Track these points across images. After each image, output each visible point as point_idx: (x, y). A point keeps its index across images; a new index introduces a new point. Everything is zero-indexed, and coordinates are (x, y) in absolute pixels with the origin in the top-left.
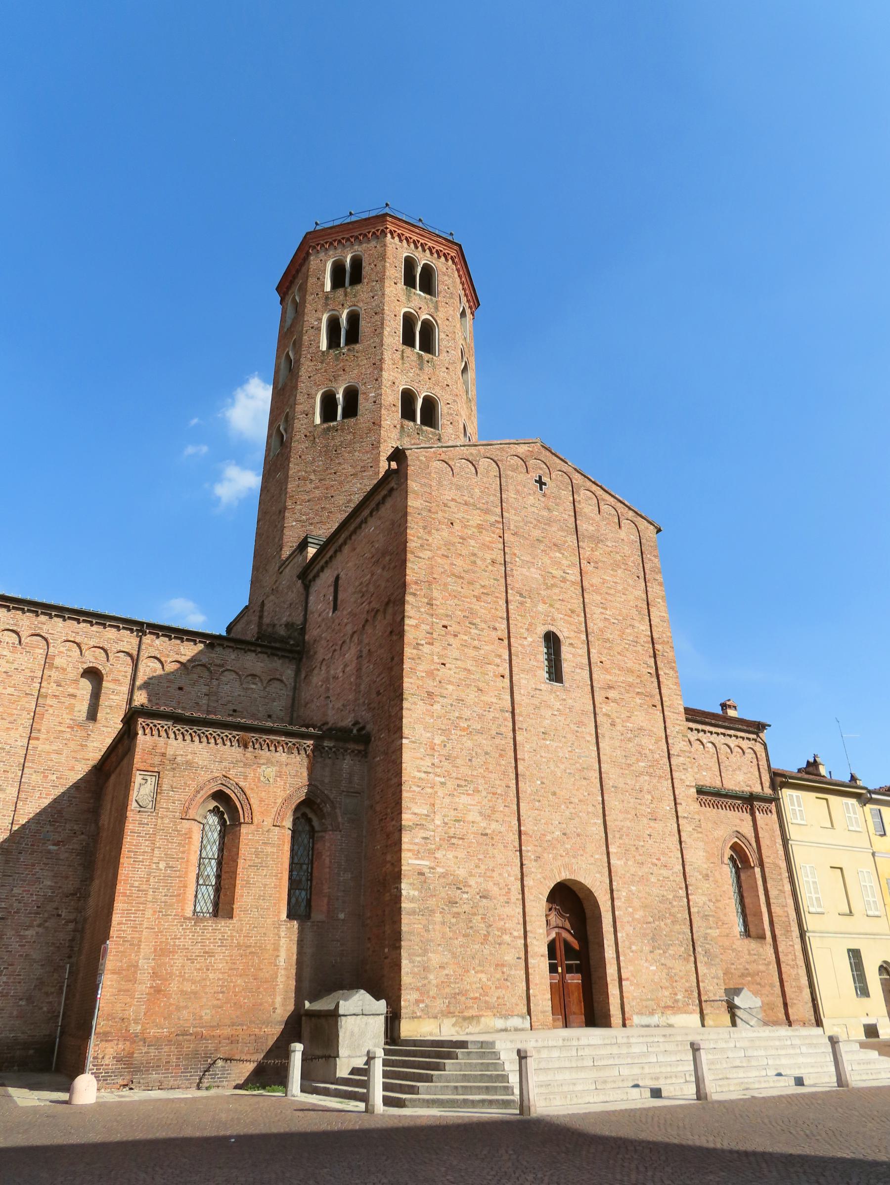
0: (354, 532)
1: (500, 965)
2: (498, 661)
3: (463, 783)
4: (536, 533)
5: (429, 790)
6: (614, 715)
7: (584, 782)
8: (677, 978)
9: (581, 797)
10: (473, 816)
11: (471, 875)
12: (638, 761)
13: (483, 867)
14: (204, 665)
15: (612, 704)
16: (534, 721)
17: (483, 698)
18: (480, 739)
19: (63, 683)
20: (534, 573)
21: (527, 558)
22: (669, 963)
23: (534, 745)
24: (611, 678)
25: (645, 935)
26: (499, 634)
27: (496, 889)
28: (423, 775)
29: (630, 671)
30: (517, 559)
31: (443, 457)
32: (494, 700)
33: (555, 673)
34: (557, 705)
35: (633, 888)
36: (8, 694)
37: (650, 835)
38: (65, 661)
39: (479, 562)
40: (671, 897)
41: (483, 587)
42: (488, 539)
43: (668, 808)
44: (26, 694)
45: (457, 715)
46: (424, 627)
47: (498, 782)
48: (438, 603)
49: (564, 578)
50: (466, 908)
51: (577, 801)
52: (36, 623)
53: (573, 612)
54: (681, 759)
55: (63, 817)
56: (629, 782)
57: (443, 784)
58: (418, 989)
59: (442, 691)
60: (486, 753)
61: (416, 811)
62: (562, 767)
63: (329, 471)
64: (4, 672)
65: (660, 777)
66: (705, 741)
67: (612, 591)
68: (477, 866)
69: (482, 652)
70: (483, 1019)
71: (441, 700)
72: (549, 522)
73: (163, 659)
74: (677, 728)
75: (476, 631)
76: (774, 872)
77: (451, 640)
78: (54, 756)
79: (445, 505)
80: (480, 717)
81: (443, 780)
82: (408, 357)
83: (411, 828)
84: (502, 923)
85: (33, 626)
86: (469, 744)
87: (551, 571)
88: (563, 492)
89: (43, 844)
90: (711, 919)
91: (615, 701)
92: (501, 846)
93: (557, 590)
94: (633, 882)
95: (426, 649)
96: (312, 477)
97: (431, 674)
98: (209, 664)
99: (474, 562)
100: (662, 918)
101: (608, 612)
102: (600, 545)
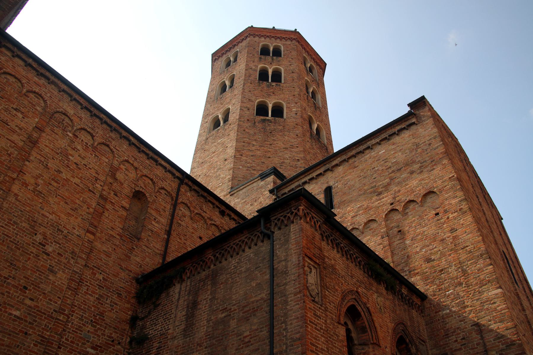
0: (354, 156)
14: (217, 226)
19: (119, 195)
36: (75, 183)
38: (123, 177)
44: (89, 190)
52: (108, 135)
55: (104, 320)
63: (267, 143)
64: (75, 163)
73: (192, 209)
78: (103, 256)
85: (105, 137)
89: (83, 343)
96: (254, 143)
98: (222, 227)
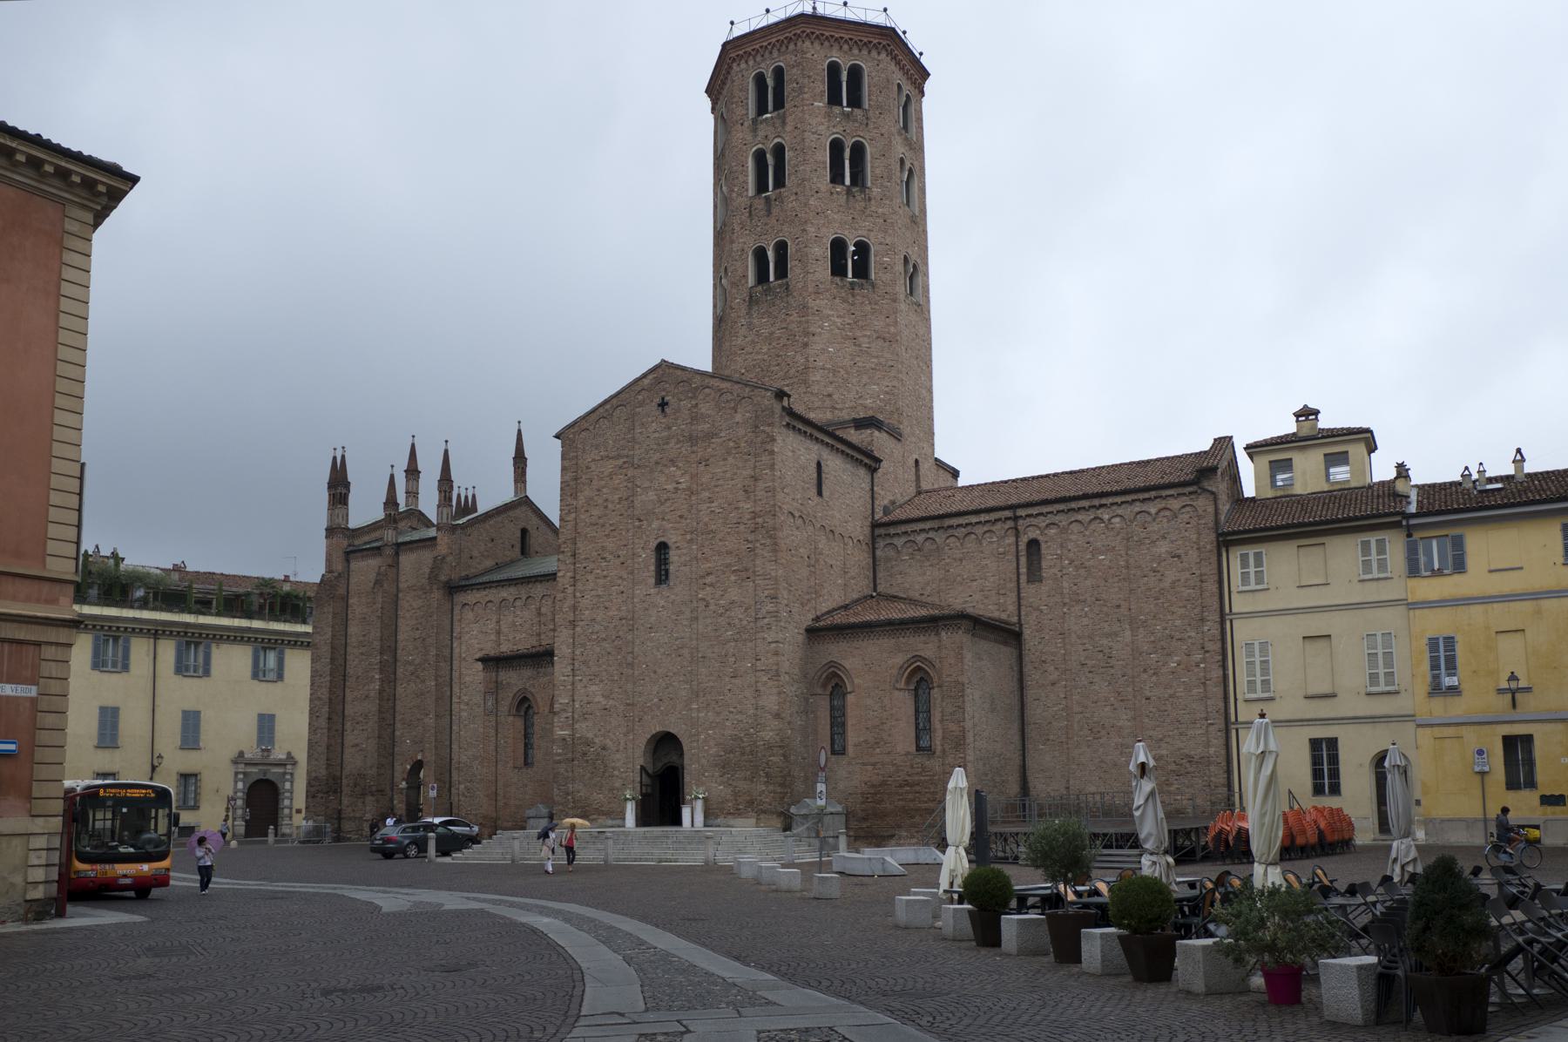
1: (612, 790)
2: (620, 582)
3: (593, 677)
4: (657, 456)
5: (570, 687)
6: (708, 598)
7: (679, 659)
8: (740, 794)
9: (675, 670)
10: (599, 698)
11: (596, 736)
12: (727, 631)
13: (603, 730)
15: (708, 589)
16: (642, 621)
17: (608, 614)
18: (605, 645)
20: (652, 495)
21: (647, 484)
22: (734, 784)
23: (642, 639)
24: (709, 565)
25: (716, 765)
26: (622, 559)
27: (610, 743)
28: (566, 678)
29: (729, 553)
30: (638, 489)
31: (586, 425)
32: (616, 613)
33: (662, 576)
34: (662, 603)
35: (711, 732)
37: (730, 690)
39: (610, 506)
40: (742, 735)
41: (611, 525)
42: (617, 481)
43: (749, 665)
45: (590, 631)
46: (569, 574)
47: (615, 672)
48: (581, 551)
49: (676, 489)
50: (592, 757)
51: (671, 674)
53: (681, 517)
54: (766, 621)
56: (716, 650)
57: (581, 680)
58: (562, 804)
59: (583, 617)
60: (609, 653)
61: (562, 701)
62: (661, 650)
65: (745, 640)
66: (1106, 517)
67: (720, 482)
68: (600, 730)
69: (609, 579)
70: (599, 821)
71: (581, 623)
72: (667, 441)
74: (766, 593)
75: (605, 564)
76: (953, 690)
77: (591, 577)
79: (588, 468)
80: (606, 628)
81: (580, 678)
82: (756, 209)
83: (559, 712)
84: (614, 764)
86: (598, 649)
87: (666, 487)
88: (682, 403)
90: (775, 749)
91: (711, 585)
92: (615, 714)
93: (668, 504)
94: (710, 729)
95: (570, 590)
97: (574, 608)
99: (606, 507)
100: (731, 752)
101: (713, 505)
102: (713, 440)
